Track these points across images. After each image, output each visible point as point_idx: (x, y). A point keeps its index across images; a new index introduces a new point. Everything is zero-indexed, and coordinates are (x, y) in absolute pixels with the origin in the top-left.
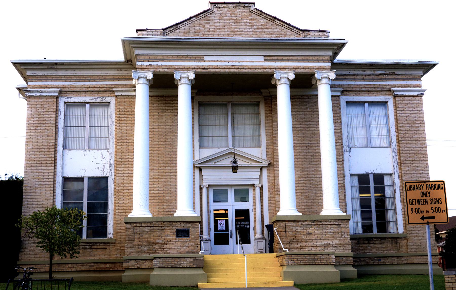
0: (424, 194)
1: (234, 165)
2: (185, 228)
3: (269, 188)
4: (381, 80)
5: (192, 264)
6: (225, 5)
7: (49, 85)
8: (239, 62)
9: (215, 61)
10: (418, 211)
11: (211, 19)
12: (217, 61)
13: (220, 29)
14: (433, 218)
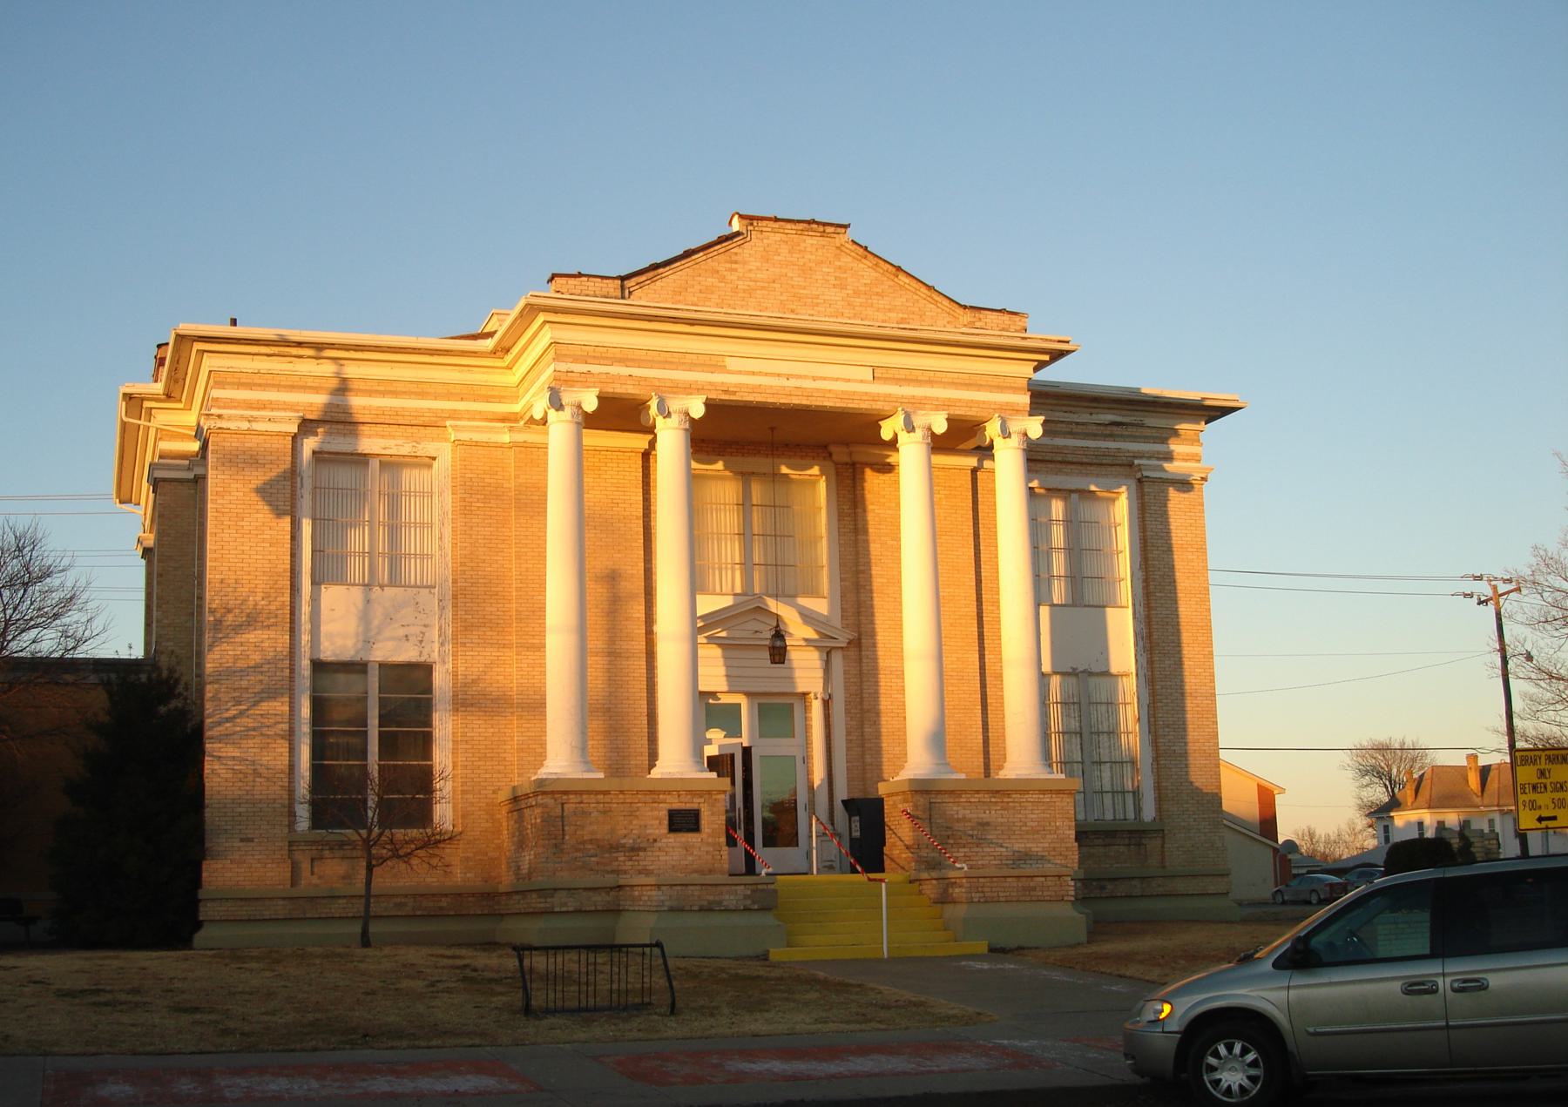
0: (1542, 773)
1: (778, 643)
2: (689, 806)
3: (847, 703)
4: (1112, 437)
5: (749, 902)
6: (777, 225)
7: (271, 402)
8: (814, 379)
9: (754, 373)
10: (1533, 806)
11: (739, 258)
12: (760, 374)
13: (763, 288)
14: (1554, 818)
